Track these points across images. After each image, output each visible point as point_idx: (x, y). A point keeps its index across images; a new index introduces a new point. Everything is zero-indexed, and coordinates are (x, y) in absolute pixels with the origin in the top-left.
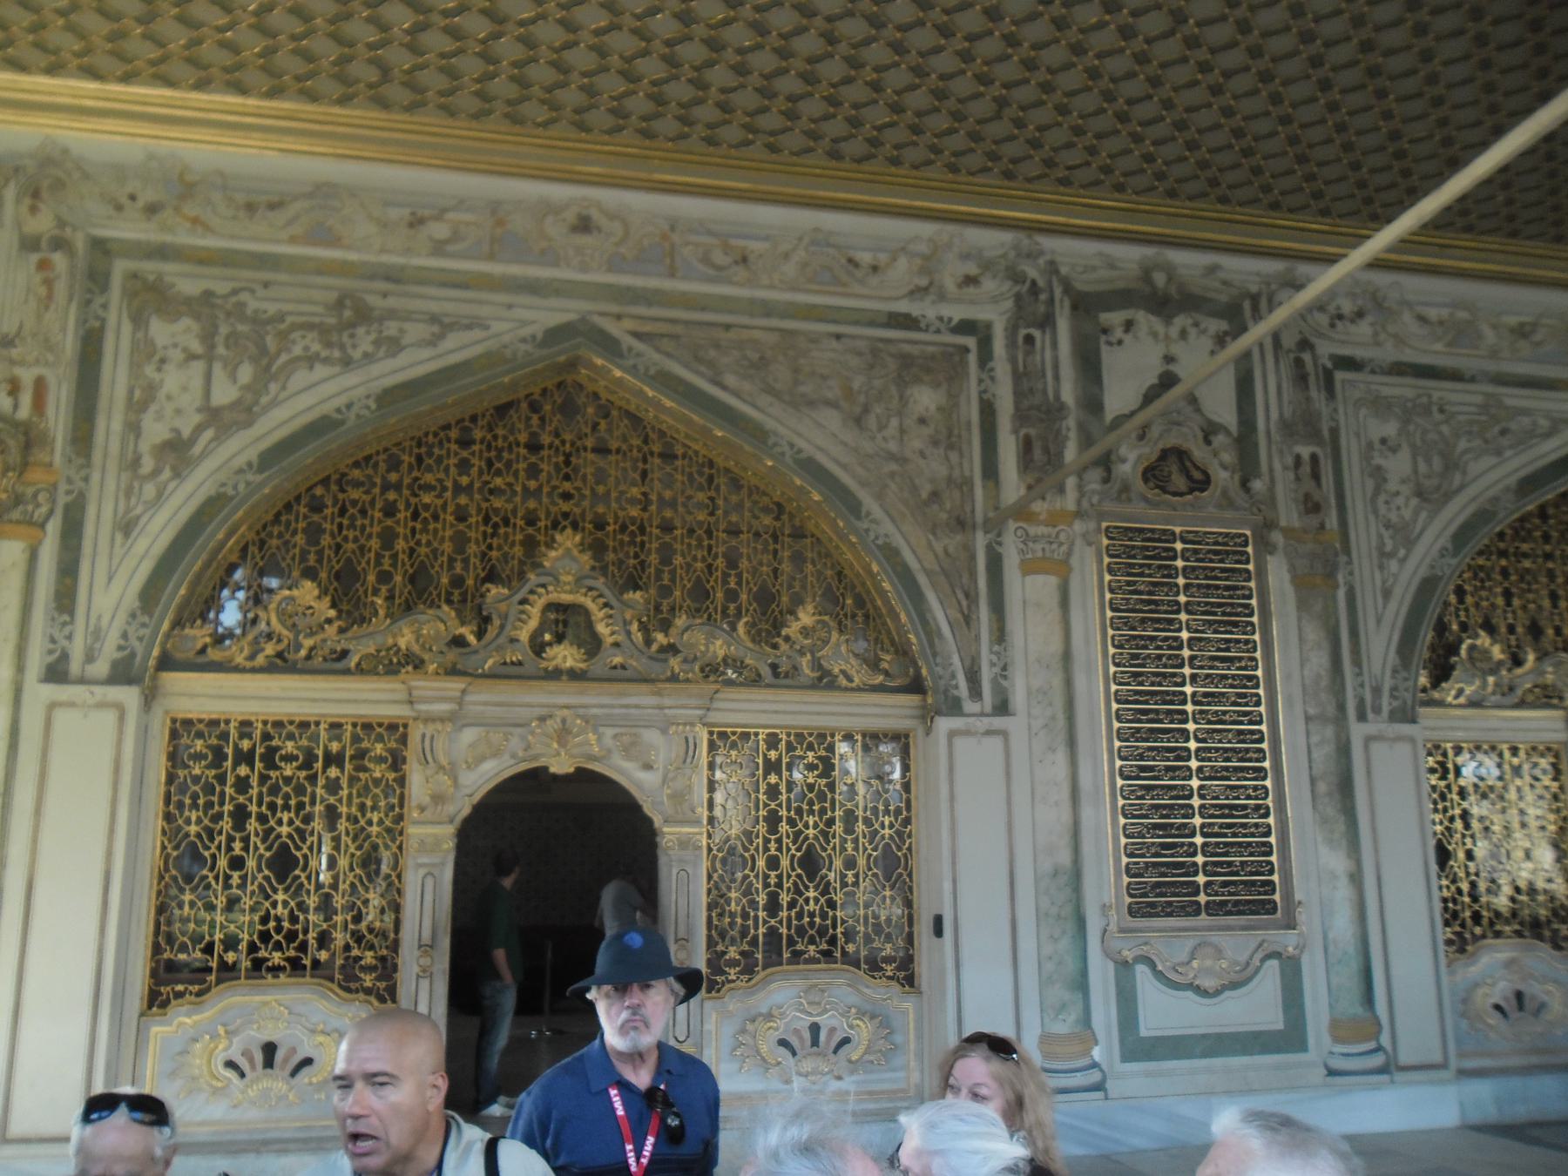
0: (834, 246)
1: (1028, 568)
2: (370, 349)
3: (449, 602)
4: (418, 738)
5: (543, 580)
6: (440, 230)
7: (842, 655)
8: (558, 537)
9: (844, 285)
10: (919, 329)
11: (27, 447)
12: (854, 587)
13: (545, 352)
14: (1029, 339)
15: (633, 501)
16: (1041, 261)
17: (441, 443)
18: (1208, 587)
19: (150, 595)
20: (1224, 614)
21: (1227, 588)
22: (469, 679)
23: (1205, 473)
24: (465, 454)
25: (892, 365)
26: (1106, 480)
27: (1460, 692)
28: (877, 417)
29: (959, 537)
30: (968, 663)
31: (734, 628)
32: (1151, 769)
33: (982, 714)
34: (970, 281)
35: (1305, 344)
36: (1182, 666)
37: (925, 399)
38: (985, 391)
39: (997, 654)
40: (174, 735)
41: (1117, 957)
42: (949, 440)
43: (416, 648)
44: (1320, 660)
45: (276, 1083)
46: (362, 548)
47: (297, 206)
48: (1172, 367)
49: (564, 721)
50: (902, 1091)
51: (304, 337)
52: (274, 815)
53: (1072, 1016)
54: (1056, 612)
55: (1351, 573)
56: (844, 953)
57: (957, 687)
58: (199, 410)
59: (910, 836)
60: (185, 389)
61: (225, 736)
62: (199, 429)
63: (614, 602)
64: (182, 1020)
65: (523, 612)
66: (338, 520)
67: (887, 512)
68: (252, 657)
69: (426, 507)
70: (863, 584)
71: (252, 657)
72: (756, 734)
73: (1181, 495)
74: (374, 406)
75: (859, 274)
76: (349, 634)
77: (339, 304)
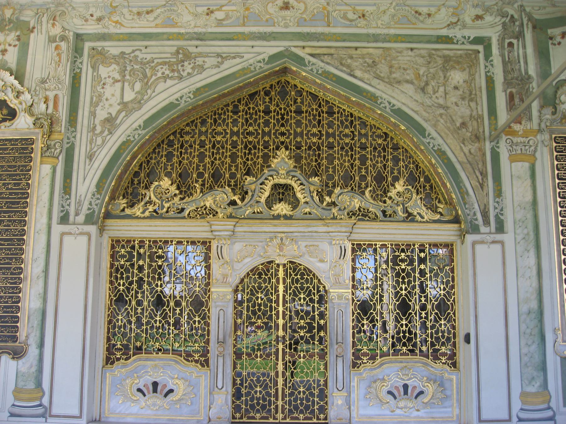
0: (408, 6)
1: (513, 159)
2: (190, 71)
3: (229, 186)
4: (215, 248)
5: (271, 173)
6: (220, 15)
7: (417, 205)
8: (278, 153)
9: (413, 24)
10: (453, 43)
11: (52, 124)
12: (424, 172)
13: (269, 66)
14: (511, 45)
15: (314, 135)
16: (516, 6)
17: (225, 113)
19: (99, 186)
22: (237, 220)
24: (235, 117)
25: (440, 61)
26: (554, 113)
28: (433, 87)
29: (477, 145)
30: (482, 208)
31: (363, 193)
33: (490, 233)
34: (479, 17)
37: (457, 77)
38: (489, 72)
39: (498, 202)
40: (113, 247)
41: (562, 355)
42: (470, 96)
43: (214, 207)
45: (157, 400)
46: (190, 162)
47: (159, 11)
49: (282, 239)
50: (450, 417)
51: (162, 68)
52: (154, 282)
53: (538, 383)
54: (529, 182)
56: (421, 351)
57: (476, 220)
58: (119, 104)
59: (454, 294)
60: (113, 95)
61: (133, 247)
62: (119, 112)
63: (305, 182)
64: (119, 370)
65: (261, 188)
66: (180, 150)
67: (438, 133)
68: (143, 212)
69: (219, 142)
70: (429, 171)
71: (143, 212)
72: (376, 245)
74: (192, 97)
75: (421, 18)
76: (184, 201)
77: (178, 52)
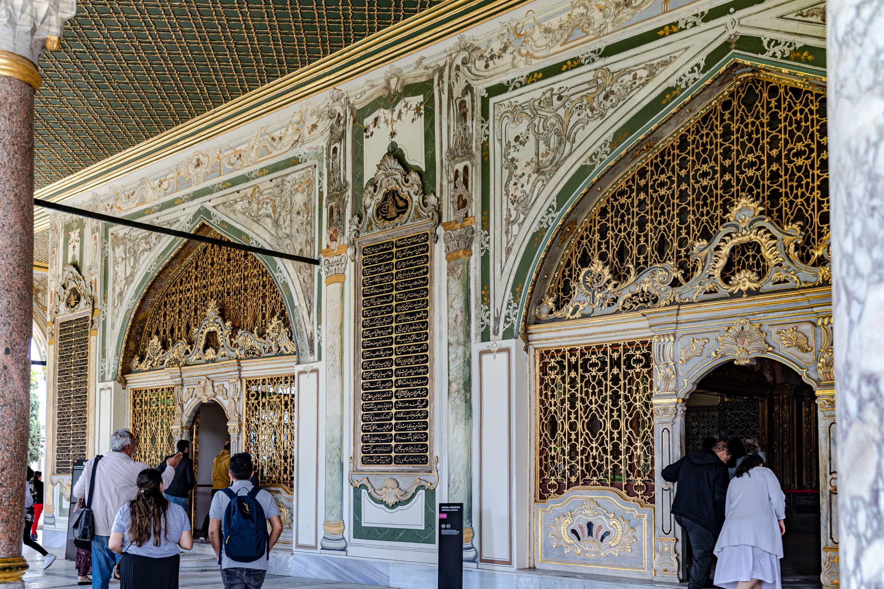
9: (270, 153)
14: (335, 149)
18: (407, 272)
20: (414, 286)
21: (416, 270)
23: (406, 201)
27: (576, 309)
29: (309, 271)
32: (375, 383)
34: (314, 126)
35: (468, 89)
36: (391, 323)
44: (458, 304)
48: (393, 140)
55: (488, 243)
73: (393, 219)
